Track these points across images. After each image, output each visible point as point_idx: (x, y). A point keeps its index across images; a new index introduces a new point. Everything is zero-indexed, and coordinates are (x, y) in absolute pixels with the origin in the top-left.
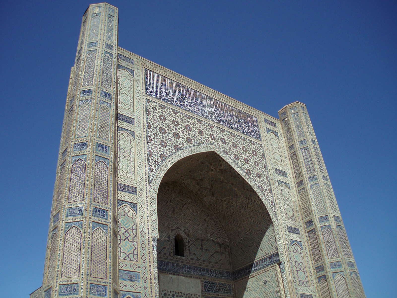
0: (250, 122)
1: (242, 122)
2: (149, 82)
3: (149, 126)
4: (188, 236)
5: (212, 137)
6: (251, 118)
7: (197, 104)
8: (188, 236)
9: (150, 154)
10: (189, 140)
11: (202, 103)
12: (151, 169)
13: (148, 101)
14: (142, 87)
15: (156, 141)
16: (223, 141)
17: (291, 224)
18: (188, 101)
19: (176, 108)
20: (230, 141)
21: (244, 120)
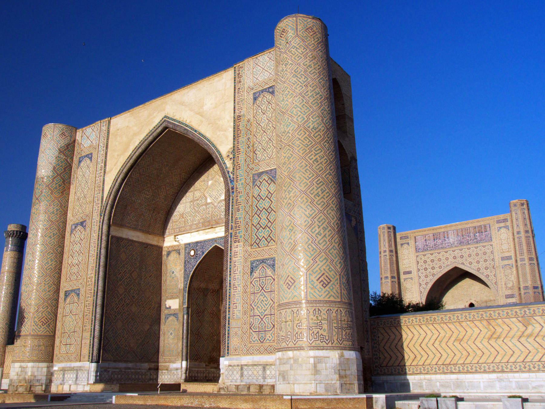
0: (483, 231)
1: (478, 234)
2: (417, 243)
3: (419, 270)
4: (477, 302)
5: (455, 258)
6: (485, 226)
7: (445, 240)
8: (477, 302)
9: (420, 285)
10: (440, 267)
11: (448, 238)
12: (421, 292)
13: (417, 256)
14: (413, 249)
15: (423, 278)
16: (462, 257)
17: (509, 292)
18: (439, 242)
19: (432, 252)
20: (465, 255)
21: (479, 232)
